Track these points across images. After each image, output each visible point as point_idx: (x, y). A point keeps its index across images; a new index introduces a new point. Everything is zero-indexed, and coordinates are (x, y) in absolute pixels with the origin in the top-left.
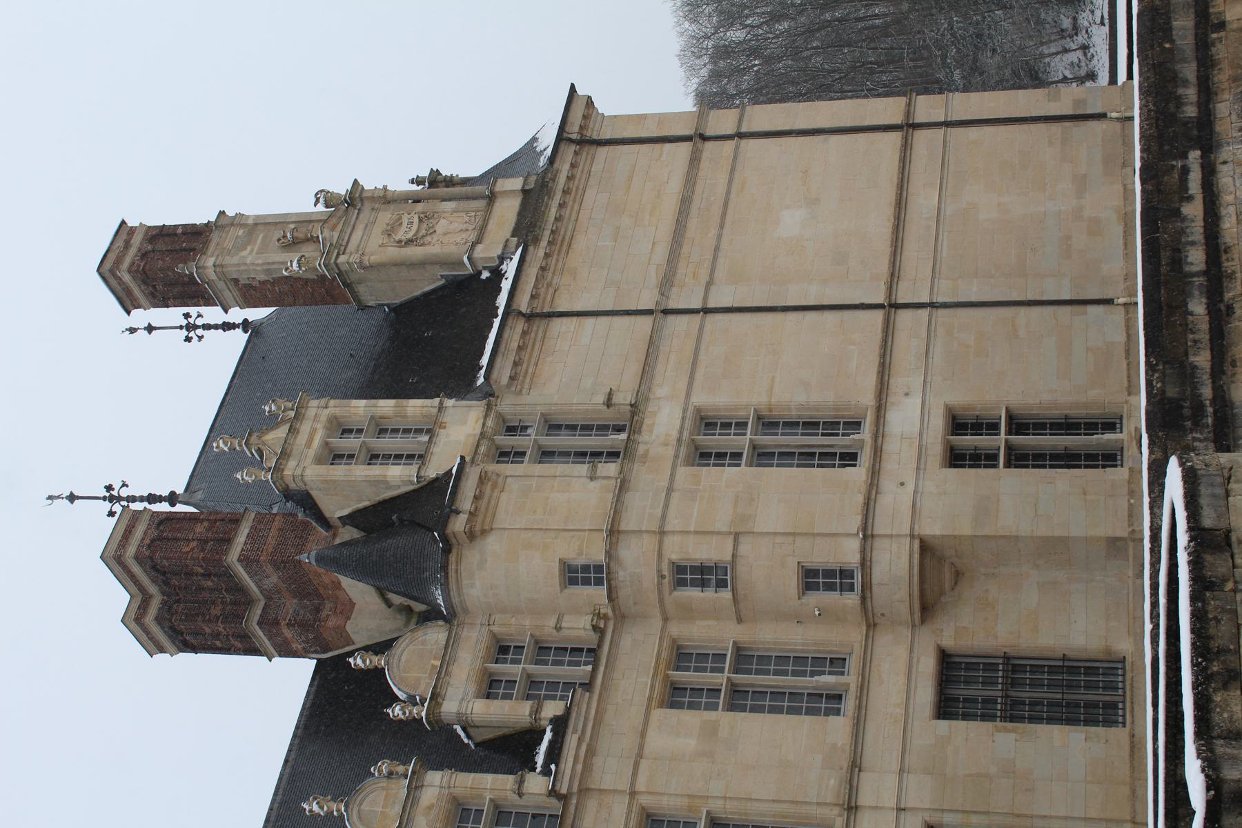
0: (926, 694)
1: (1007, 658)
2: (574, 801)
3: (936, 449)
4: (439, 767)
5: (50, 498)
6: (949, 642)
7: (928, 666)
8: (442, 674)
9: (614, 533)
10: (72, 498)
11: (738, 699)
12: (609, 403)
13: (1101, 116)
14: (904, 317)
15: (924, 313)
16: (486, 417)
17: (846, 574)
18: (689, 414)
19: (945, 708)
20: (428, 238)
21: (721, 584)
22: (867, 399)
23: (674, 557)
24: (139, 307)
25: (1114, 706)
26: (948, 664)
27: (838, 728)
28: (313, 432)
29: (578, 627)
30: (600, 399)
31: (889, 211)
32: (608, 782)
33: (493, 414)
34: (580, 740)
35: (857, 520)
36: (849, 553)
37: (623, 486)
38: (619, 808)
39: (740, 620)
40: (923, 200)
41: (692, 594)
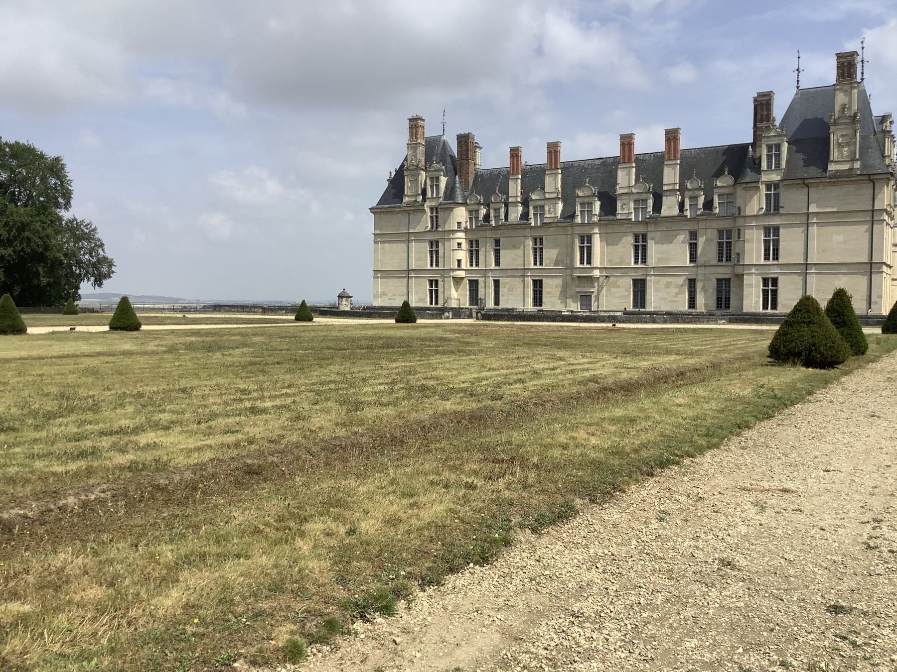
0: (720, 277)
7: (726, 277)
10: (799, 57)
13: (870, 308)
22: (781, 261)
25: (721, 307)
38: (696, 227)
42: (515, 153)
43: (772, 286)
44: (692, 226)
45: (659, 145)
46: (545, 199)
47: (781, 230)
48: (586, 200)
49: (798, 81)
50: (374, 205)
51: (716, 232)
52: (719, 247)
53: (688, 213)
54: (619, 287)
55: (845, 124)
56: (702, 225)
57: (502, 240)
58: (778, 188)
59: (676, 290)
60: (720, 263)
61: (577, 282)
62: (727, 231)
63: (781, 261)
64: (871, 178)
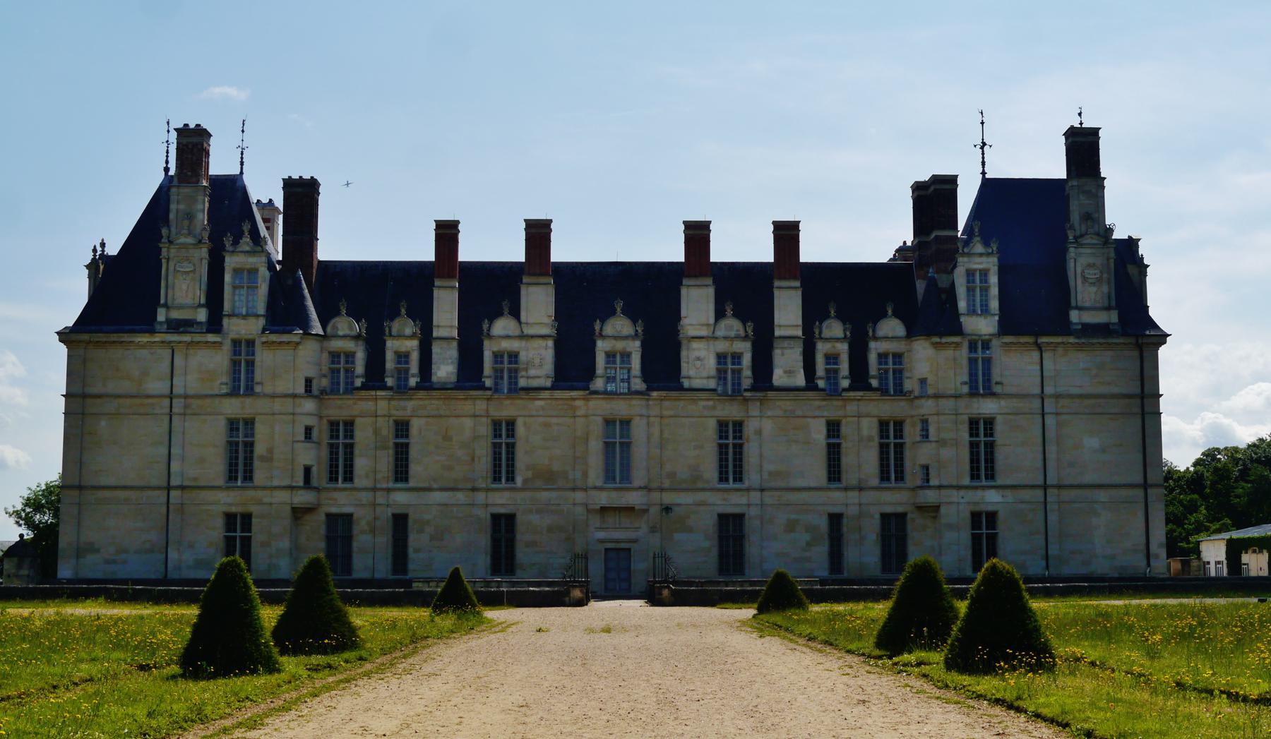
1: (906, 535)
2: (840, 398)
3: (977, 509)
4: (850, 347)
5: (982, 113)
6: (909, 516)
7: (900, 509)
8: (886, 338)
9: (937, 396)
10: (982, 123)
11: (883, 448)
12: (997, 383)
14: (1040, 493)
15: (1042, 500)
16: (990, 335)
17: (928, 481)
18: (993, 416)
19: (885, 517)
20: (1087, 284)
21: (922, 436)
22: (999, 482)
23: (930, 420)
24: (1066, 139)
26: (901, 517)
27: (875, 481)
28: (981, 263)
29: (908, 385)
30: (998, 379)
31: (1098, 482)
32: (848, 408)
33: (991, 337)
34: (862, 396)
35: (945, 483)
36: (934, 482)
37: (956, 397)
38: (840, 413)
39: (914, 443)
40: (1102, 495)
41: (919, 427)
42: (447, 233)
43: (987, 529)
44: (833, 409)
45: (763, 251)
46: (523, 337)
47: (999, 427)
48: (619, 345)
49: (983, 163)
50: (70, 323)
51: (875, 422)
52: (721, 453)
53: (821, 384)
54: (690, 530)
55: (1092, 246)
56: (852, 408)
57: (416, 424)
58: (988, 348)
59: (807, 537)
60: (886, 485)
61: (595, 521)
62: (895, 423)
63: (999, 482)
64: (1140, 341)
